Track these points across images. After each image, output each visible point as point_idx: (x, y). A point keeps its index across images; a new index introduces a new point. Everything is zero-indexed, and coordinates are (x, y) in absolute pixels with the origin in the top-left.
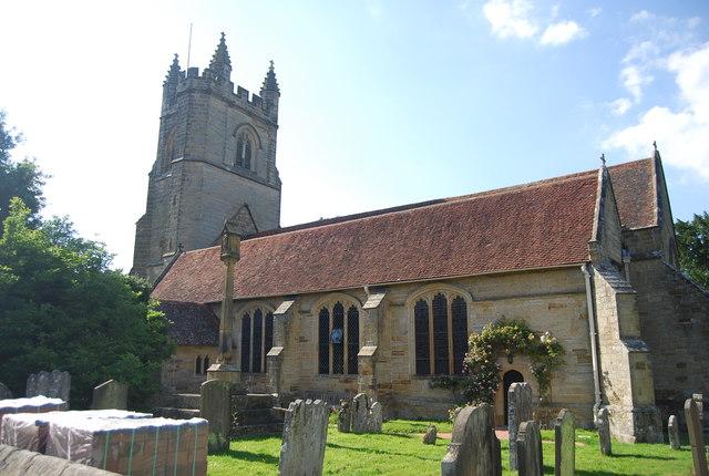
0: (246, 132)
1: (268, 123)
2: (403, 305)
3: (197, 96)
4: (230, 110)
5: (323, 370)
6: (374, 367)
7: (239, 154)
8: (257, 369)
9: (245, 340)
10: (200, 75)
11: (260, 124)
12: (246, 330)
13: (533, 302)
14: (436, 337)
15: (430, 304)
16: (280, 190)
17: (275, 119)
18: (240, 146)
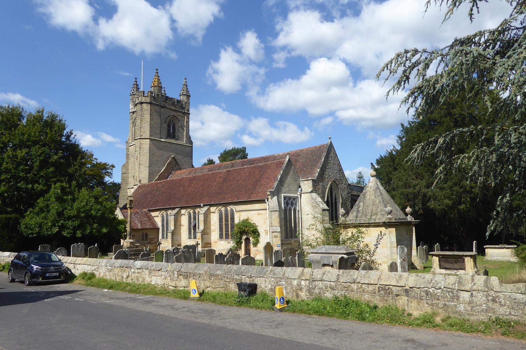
0: (172, 119)
1: (184, 113)
2: (214, 212)
3: (144, 105)
4: (162, 110)
5: (190, 238)
6: (202, 237)
7: (169, 130)
8: (167, 238)
9: (163, 225)
10: (146, 95)
11: (179, 114)
12: (163, 221)
13: (253, 212)
14: (225, 225)
15: (223, 212)
16: (192, 147)
17: (188, 110)
18: (169, 126)
